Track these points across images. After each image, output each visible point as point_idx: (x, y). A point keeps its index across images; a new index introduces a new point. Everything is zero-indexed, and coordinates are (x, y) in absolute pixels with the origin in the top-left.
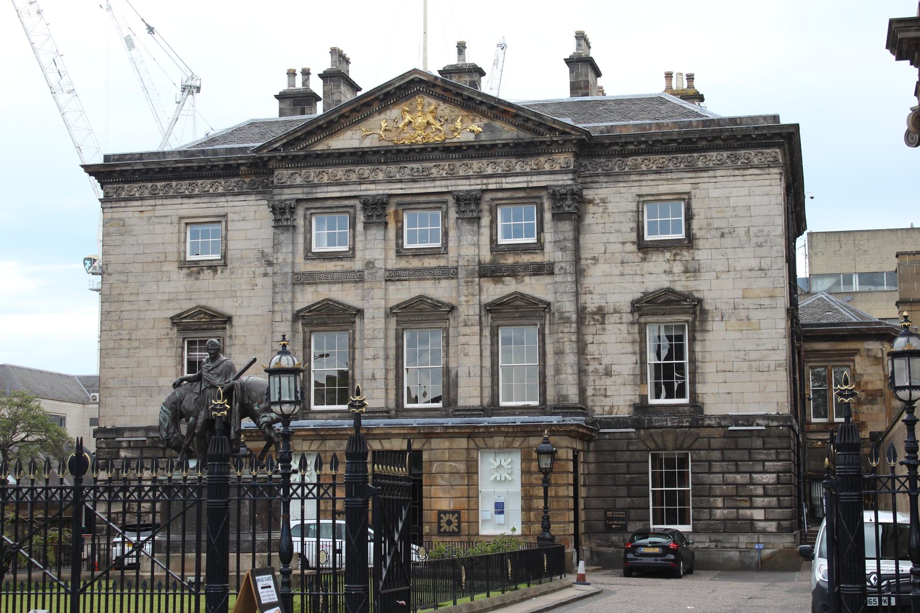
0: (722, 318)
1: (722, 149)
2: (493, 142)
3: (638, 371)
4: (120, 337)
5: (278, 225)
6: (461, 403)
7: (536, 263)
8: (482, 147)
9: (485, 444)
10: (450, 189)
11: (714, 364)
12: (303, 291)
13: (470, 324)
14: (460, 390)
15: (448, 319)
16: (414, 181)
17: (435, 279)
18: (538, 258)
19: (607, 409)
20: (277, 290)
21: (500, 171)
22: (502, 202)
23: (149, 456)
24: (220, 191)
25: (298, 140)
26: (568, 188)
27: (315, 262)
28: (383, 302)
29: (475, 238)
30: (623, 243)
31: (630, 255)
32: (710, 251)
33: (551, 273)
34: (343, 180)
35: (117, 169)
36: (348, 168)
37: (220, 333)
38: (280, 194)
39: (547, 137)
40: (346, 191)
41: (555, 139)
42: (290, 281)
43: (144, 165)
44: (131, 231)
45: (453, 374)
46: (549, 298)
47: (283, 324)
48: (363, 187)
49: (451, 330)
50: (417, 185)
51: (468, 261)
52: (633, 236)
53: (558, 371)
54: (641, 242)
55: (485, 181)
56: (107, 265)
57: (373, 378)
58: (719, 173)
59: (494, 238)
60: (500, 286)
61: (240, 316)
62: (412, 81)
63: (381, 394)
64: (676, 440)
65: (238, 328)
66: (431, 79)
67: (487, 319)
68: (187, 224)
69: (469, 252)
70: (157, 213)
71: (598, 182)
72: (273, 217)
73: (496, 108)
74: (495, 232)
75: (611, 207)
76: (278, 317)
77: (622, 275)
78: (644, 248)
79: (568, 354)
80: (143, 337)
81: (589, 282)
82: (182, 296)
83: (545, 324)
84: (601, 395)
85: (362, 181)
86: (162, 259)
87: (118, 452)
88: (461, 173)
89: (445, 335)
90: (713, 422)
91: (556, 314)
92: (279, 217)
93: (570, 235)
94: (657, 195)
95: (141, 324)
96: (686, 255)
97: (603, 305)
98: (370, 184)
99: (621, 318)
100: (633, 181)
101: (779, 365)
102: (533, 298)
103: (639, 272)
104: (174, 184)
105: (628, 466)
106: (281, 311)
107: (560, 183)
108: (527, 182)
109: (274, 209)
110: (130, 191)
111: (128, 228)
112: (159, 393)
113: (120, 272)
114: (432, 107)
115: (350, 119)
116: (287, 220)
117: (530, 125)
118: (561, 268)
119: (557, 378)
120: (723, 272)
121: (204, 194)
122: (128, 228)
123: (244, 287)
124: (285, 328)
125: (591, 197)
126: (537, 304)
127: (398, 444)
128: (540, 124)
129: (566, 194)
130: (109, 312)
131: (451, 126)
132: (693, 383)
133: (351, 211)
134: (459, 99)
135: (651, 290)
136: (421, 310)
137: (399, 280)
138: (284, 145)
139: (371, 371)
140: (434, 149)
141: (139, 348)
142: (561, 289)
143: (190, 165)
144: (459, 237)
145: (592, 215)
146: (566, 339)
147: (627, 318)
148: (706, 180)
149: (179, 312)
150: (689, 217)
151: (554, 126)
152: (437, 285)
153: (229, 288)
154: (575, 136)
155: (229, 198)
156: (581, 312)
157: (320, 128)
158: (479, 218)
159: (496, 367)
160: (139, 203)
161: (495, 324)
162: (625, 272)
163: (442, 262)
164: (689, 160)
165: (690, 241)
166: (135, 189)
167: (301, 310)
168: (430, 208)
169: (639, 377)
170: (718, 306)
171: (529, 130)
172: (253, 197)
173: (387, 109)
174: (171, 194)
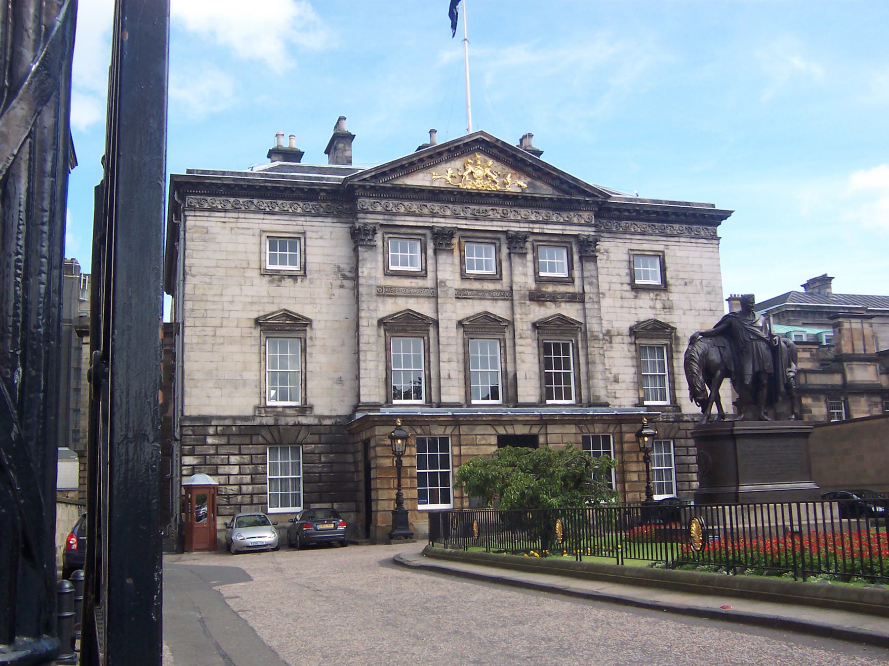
4: (205, 333)
6: (521, 400)
7: (569, 293)
8: (534, 199)
9: (588, 430)
10: (505, 229)
12: (383, 301)
13: (524, 336)
14: (519, 389)
16: (477, 219)
17: (493, 299)
18: (570, 289)
21: (541, 219)
22: (542, 243)
23: (236, 442)
24: (298, 212)
25: (384, 174)
26: (593, 237)
27: (395, 278)
30: (622, 284)
31: (626, 293)
35: (207, 181)
36: (423, 203)
37: (301, 335)
39: (581, 198)
41: (587, 199)
42: (374, 292)
43: (233, 181)
44: (214, 238)
45: (511, 375)
46: (580, 320)
47: (370, 328)
48: (435, 220)
49: (509, 343)
52: (627, 279)
53: (589, 377)
55: (531, 225)
56: (190, 267)
57: (449, 377)
58: (682, 239)
59: (537, 271)
60: (543, 309)
61: (319, 321)
63: (454, 390)
64: (665, 430)
66: (493, 141)
68: (268, 237)
70: (239, 225)
75: (612, 256)
77: (622, 307)
78: (637, 289)
79: (598, 363)
80: (227, 334)
82: (266, 300)
84: (612, 397)
85: (433, 215)
86: (245, 265)
87: (206, 439)
89: (502, 345)
90: (689, 419)
91: (588, 333)
93: (594, 273)
95: (225, 324)
96: (663, 296)
99: (623, 339)
100: (626, 239)
102: (572, 320)
103: (633, 306)
104: (255, 201)
107: (586, 233)
108: (562, 230)
113: (203, 275)
115: (424, 163)
116: (370, 240)
117: (565, 187)
118: (590, 298)
121: (284, 212)
124: (370, 333)
128: (576, 187)
129: (591, 242)
130: (193, 310)
133: (423, 238)
134: (511, 160)
135: (642, 320)
139: (447, 372)
141: (223, 344)
143: (278, 185)
146: (596, 352)
147: (628, 340)
148: (674, 243)
149: (262, 314)
150: (663, 269)
152: (495, 304)
153: (309, 296)
155: (308, 218)
157: (402, 167)
158: (526, 253)
160: (222, 214)
162: (624, 306)
163: (498, 286)
165: (664, 286)
166: (218, 202)
168: (487, 243)
170: (686, 335)
172: (329, 220)
173: (452, 160)
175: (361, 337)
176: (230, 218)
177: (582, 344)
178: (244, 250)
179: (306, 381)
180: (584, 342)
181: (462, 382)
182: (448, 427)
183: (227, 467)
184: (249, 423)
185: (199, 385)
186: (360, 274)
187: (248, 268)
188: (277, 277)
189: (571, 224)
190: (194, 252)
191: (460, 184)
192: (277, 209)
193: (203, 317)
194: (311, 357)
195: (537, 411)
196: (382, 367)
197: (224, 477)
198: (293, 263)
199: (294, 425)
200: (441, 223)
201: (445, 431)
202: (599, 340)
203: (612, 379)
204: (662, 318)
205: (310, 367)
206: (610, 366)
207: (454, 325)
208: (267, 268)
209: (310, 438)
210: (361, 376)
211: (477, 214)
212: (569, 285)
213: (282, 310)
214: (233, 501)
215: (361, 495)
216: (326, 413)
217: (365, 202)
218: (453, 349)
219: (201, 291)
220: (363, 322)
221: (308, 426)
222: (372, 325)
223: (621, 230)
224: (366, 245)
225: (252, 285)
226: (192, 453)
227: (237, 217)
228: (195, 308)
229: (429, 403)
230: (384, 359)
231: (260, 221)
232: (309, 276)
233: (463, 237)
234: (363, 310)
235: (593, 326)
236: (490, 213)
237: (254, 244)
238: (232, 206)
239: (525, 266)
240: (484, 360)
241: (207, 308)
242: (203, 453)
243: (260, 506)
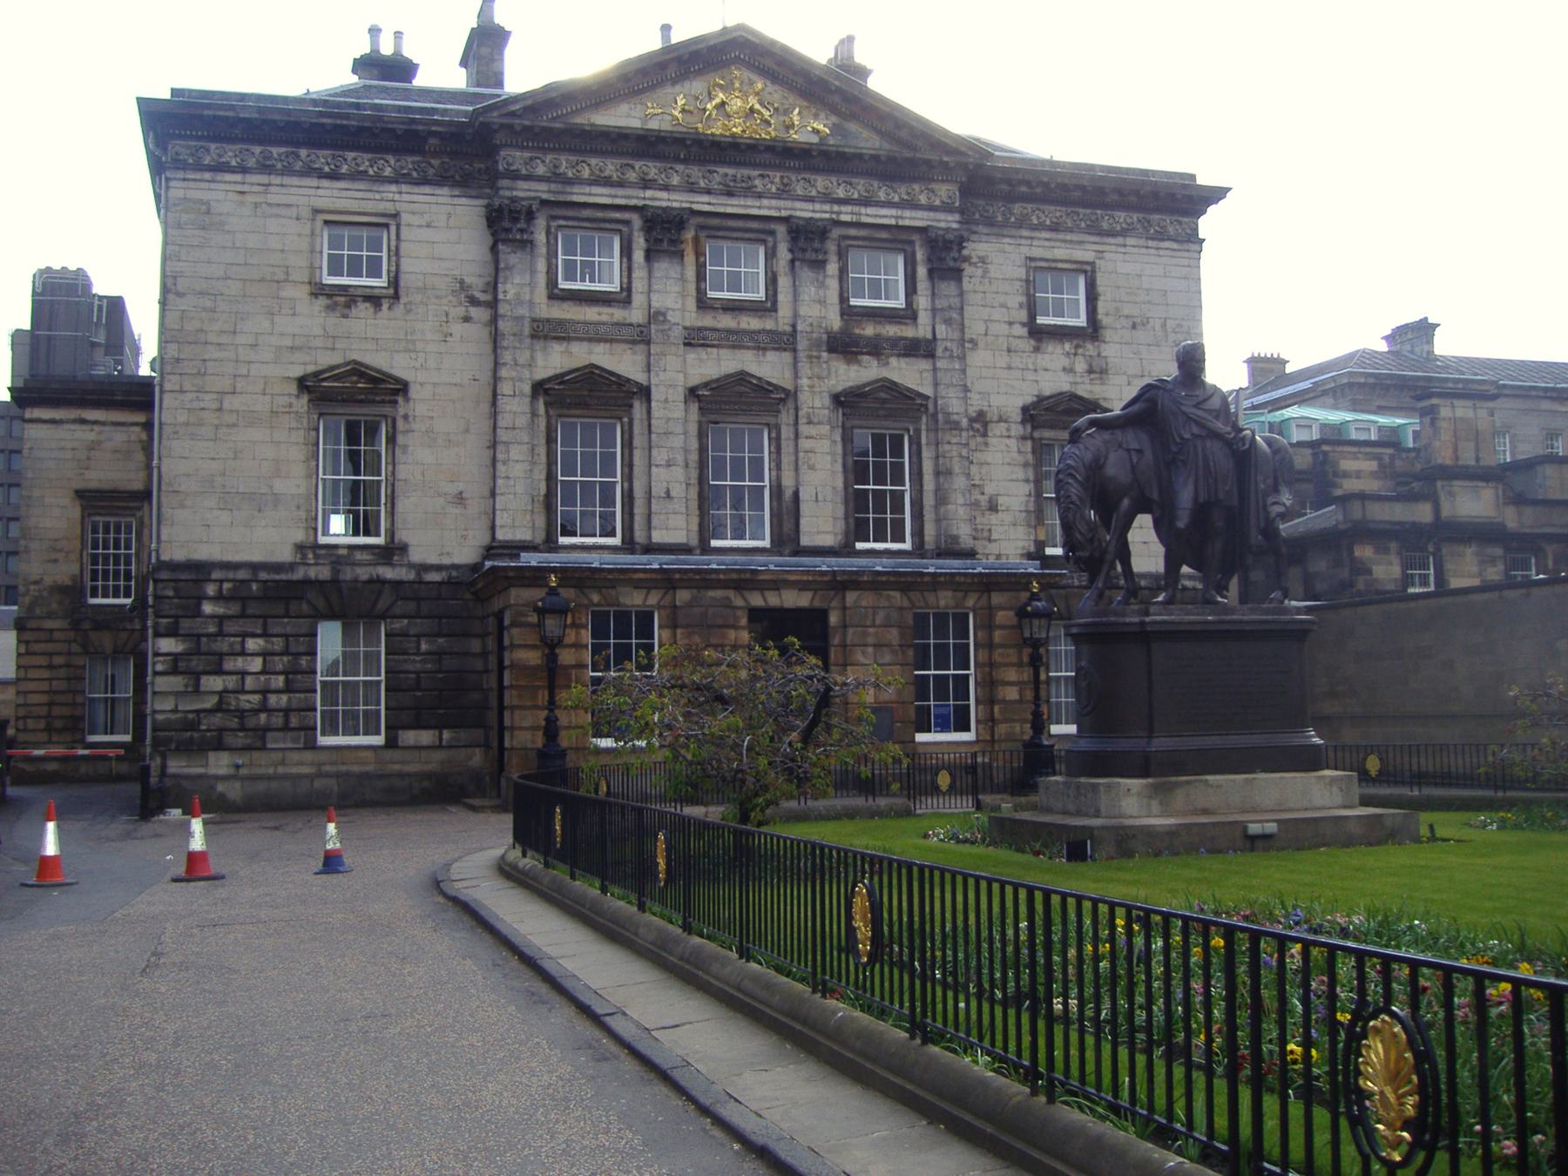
3: (1031, 507)
4: (202, 405)
6: (805, 541)
7: (905, 339)
8: (842, 156)
10: (784, 213)
12: (545, 348)
13: (816, 420)
14: (803, 521)
16: (730, 194)
17: (758, 348)
18: (908, 332)
21: (856, 196)
24: (386, 174)
26: (956, 233)
27: (566, 305)
28: (681, 376)
30: (1011, 324)
31: (1018, 341)
32: (1118, 346)
33: (931, 356)
35: (206, 112)
36: (625, 162)
37: (387, 410)
40: (620, 197)
41: (945, 159)
42: (527, 331)
43: (259, 113)
45: (788, 494)
46: (927, 390)
47: (517, 399)
48: (649, 193)
49: (787, 432)
50: (734, 201)
51: (811, 325)
52: (1023, 315)
53: (941, 499)
55: (836, 208)
56: (175, 278)
57: (668, 495)
58: (1130, 241)
60: (854, 368)
63: (679, 521)
65: (420, 404)
68: (326, 222)
69: (810, 311)
70: (272, 199)
75: (994, 271)
77: (1009, 368)
78: (1039, 334)
82: (319, 343)
85: (646, 184)
87: (199, 605)
88: (799, 192)
89: (773, 435)
91: (940, 416)
93: (956, 301)
96: (1090, 348)
98: (660, 190)
99: (1008, 430)
100: (1021, 237)
103: (1031, 367)
104: (303, 152)
106: (512, 379)
107: (943, 225)
108: (897, 217)
110: (220, 156)
112: (276, 506)
116: (522, 231)
118: (946, 349)
119: (942, 510)
120: (1136, 376)
121: (357, 175)
123: (429, 336)
124: (516, 408)
126: (913, 399)
127: (793, 599)
129: (951, 242)
130: (178, 360)
133: (625, 229)
135: (1047, 393)
136: (741, 394)
137: (703, 345)
139: (665, 484)
141: (234, 425)
143: (345, 122)
146: (955, 454)
147: (1017, 430)
149: (311, 369)
150: (1092, 298)
152: (761, 358)
155: (404, 188)
160: (238, 177)
161: (848, 424)
163: (769, 324)
164: (1093, 218)
165: (1093, 330)
166: (230, 154)
167: (549, 380)
172: (445, 191)
174: (297, 168)
175: (499, 417)
176: (252, 184)
178: (280, 247)
179: (393, 498)
180: (932, 435)
181: (694, 504)
182: (653, 592)
183: (240, 659)
184: (283, 577)
185: (188, 503)
186: (501, 296)
187: (286, 281)
188: (342, 300)
189: (912, 205)
191: (700, 125)
193: (199, 373)
194: (405, 451)
195: (825, 564)
196: (540, 474)
197: (234, 677)
198: (374, 272)
199: (370, 581)
200: (660, 200)
201: (646, 599)
202: (962, 430)
203: (984, 504)
204: (1085, 390)
205: (403, 470)
206: (981, 479)
207: (679, 395)
208: (324, 282)
209: (400, 607)
210: (498, 491)
211: (732, 184)
212: (906, 324)
213: (349, 363)
214: (251, 722)
215: (492, 717)
216: (433, 559)
217: (514, 158)
218: (677, 442)
220: (505, 388)
221: (397, 584)
222: (522, 394)
223: (1013, 219)
224: (510, 241)
225: (294, 315)
226: (172, 632)
227: (266, 182)
228: (182, 356)
229: (629, 545)
230: (543, 459)
231: (312, 192)
232: (403, 300)
233: (702, 227)
234: (505, 364)
235: (953, 404)
236: (757, 182)
237: (299, 235)
238: (258, 161)
239: (822, 285)
240: (738, 464)
241: (206, 357)
242: (195, 632)
243: (302, 733)
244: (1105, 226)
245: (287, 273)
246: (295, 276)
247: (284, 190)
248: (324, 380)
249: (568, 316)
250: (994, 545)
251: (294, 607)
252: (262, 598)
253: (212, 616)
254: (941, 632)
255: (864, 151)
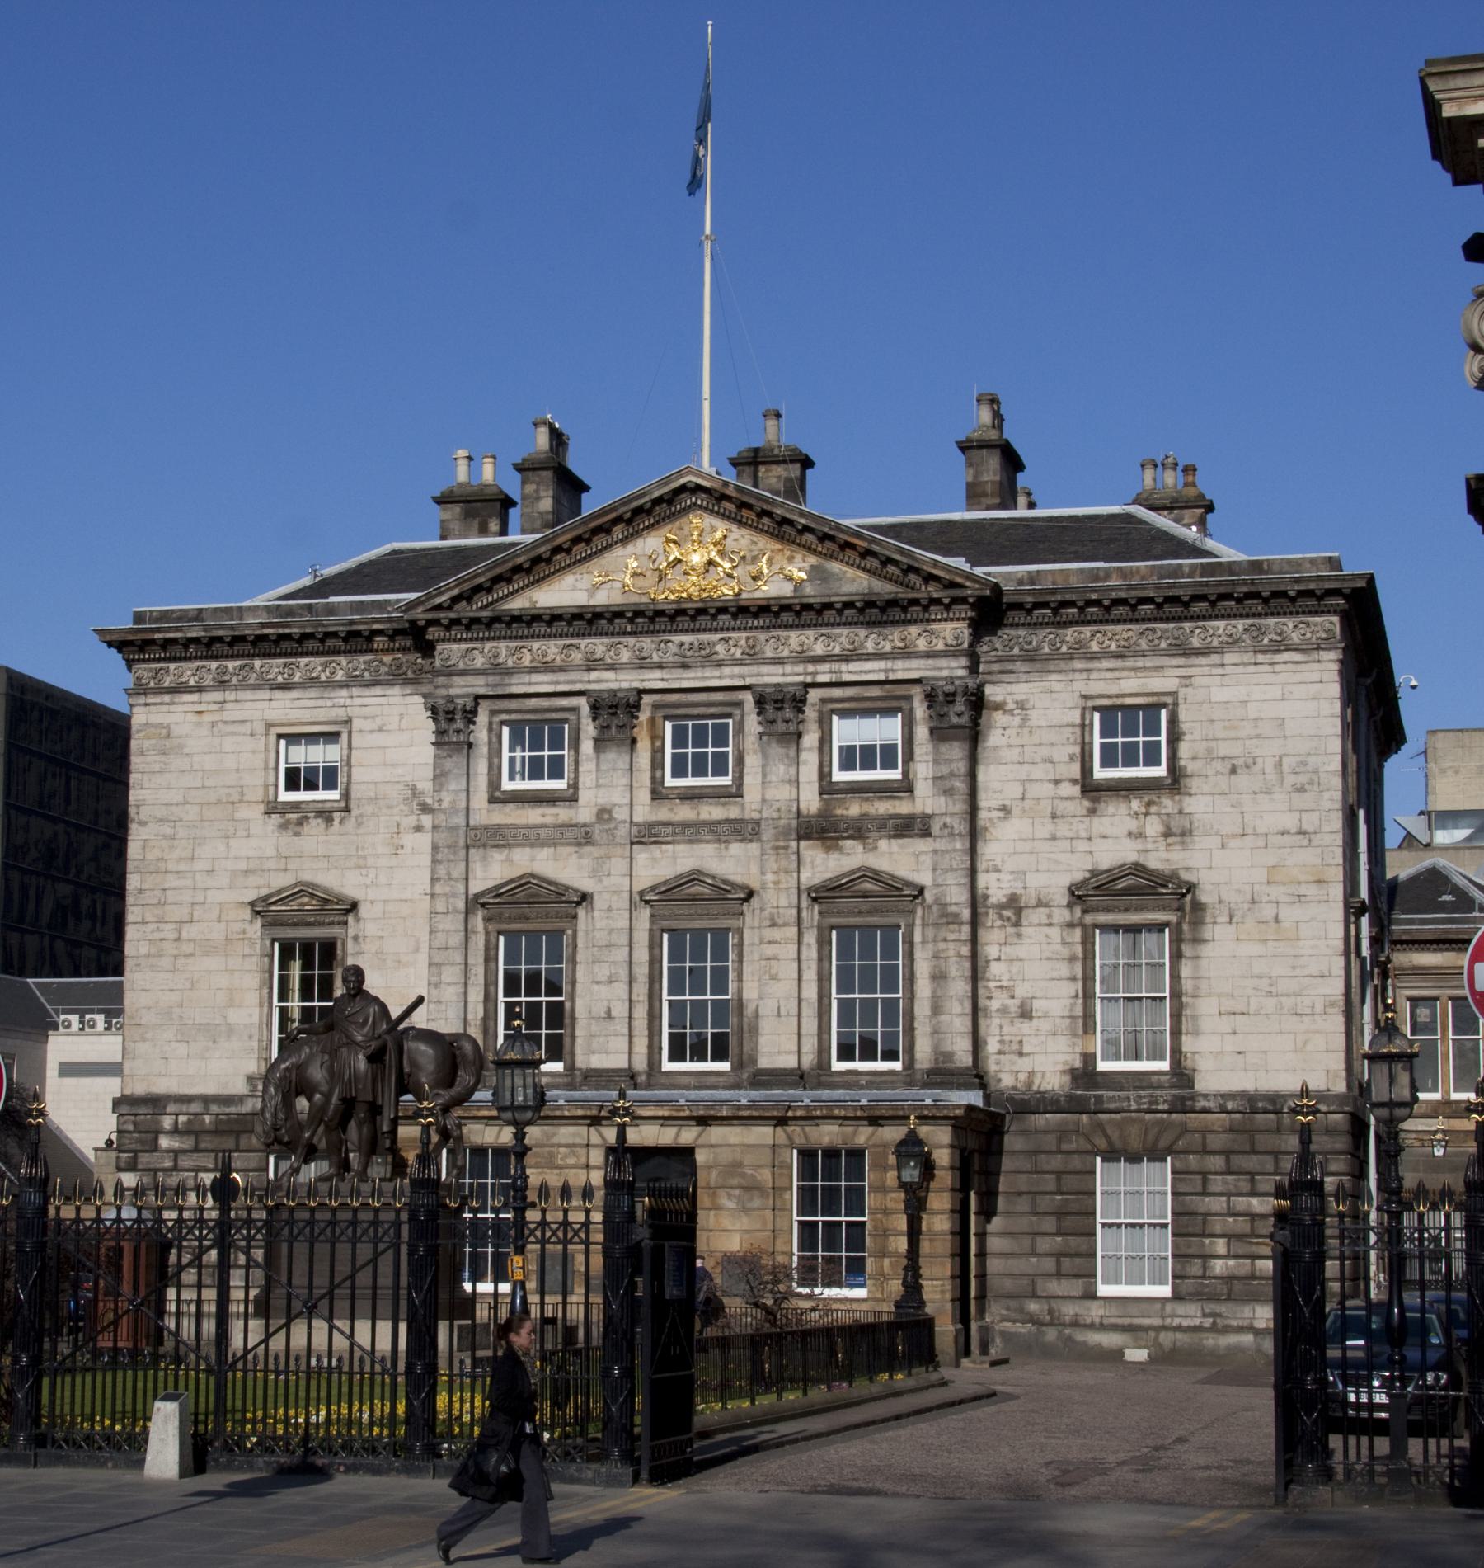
0: (1231, 917)
1: (1235, 616)
2: (826, 600)
4: (161, 935)
5: (442, 740)
8: (807, 607)
10: (748, 681)
11: (1214, 1001)
12: (484, 858)
13: (780, 921)
14: (762, 1040)
15: (742, 913)
16: (685, 666)
17: (719, 841)
18: (903, 807)
19: (1022, 1077)
20: (439, 857)
21: (837, 651)
23: (209, 1146)
29: (793, 770)
30: (1057, 782)
31: (1068, 804)
32: (1210, 798)
33: (926, 833)
34: (558, 662)
35: (157, 636)
37: (335, 931)
38: (447, 687)
41: (935, 595)
42: (462, 842)
44: (181, 747)
45: (749, 1011)
46: (924, 878)
47: (450, 917)
48: (594, 675)
51: (779, 810)
52: (1075, 770)
54: (1088, 781)
55: (811, 668)
56: (138, 806)
57: (609, 1015)
58: (1229, 658)
59: (826, 770)
60: (834, 856)
62: (683, 489)
67: (811, 914)
68: (280, 736)
69: (782, 794)
70: (227, 715)
71: (1011, 672)
72: (432, 725)
73: (832, 538)
74: (826, 759)
75: (1036, 718)
76: (440, 906)
77: (1054, 838)
81: (990, 851)
82: (271, 864)
83: (913, 924)
85: (591, 664)
86: (236, 798)
87: (156, 1139)
88: (769, 653)
90: (1212, 1105)
91: (935, 908)
92: (444, 726)
93: (961, 767)
94: (1118, 696)
96: (1168, 804)
97: (1019, 891)
99: (1049, 916)
100: (1074, 671)
101: (1332, 1005)
102: (893, 877)
104: (257, 663)
105: (1059, 1180)
106: (445, 895)
107: (945, 673)
108: (886, 671)
109: (434, 712)
111: (175, 742)
113: (161, 820)
114: (719, 535)
116: (458, 732)
118: (945, 826)
120: (1234, 836)
121: (311, 682)
122: (175, 742)
123: (380, 850)
124: (452, 925)
125: (999, 699)
128: (911, 569)
129: (954, 694)
130: (140, 891)
131: (753, 569)
132: (1176, 1033)
133: (572, 717)
134: (766, 520)
135: (1104, 866)
136: (694, 898)
137: (655, 842)
138: (455, 600)
139: (606, 1003)
140: (722, 610)
141: (192, 955)
142: (945, 863)
143: (287, 631)
144: (764, 767)
145: (1000, 731)
146: (951, 953)
147: (1061, 915)
148: (1206, 670)
149: (264, 892)
150: (1174, 738)
151: (934, 571)
152: (724, 853)
154: (971, 591)
155: (355, 691)
156: (976, 901)
158: (800, 735)
159: (825, 1001)
160: (194, 697)
162: (1059, 834)
163: (733, 812)
165: (1175, 781)
167: (482, 894)
169: (1080, 1022)
170: (1224, 897)
171: (889, 579)
172: (397, 690)
174: (252, 681)
177: (923, 934)
184: (233, 1110)
185: (149, 1035)
187: (241, 801)
188: (293, 818)
189: (906, 653)
190: (146, 777)
191: (651, 591)
192: (297, 678)
206: (1011, 979)
211: (689, 653)
217: (450, 651)
219: (156, 853)
222: (456, 911)
224: (449, 743)
232: (354, 812)
236: (720, 648)
237: (254, 752)
244: (1196, 642)
245: (242, 794)
246: (250, 796)
247: (238, 706)
248: (274, 903)
249: (509, 821)
250: (1025, 1060)
251: (244, 1141)
252: (216, 1132)
253: (168, 1151)
254: (831, 1173)
255: (833, 599)
